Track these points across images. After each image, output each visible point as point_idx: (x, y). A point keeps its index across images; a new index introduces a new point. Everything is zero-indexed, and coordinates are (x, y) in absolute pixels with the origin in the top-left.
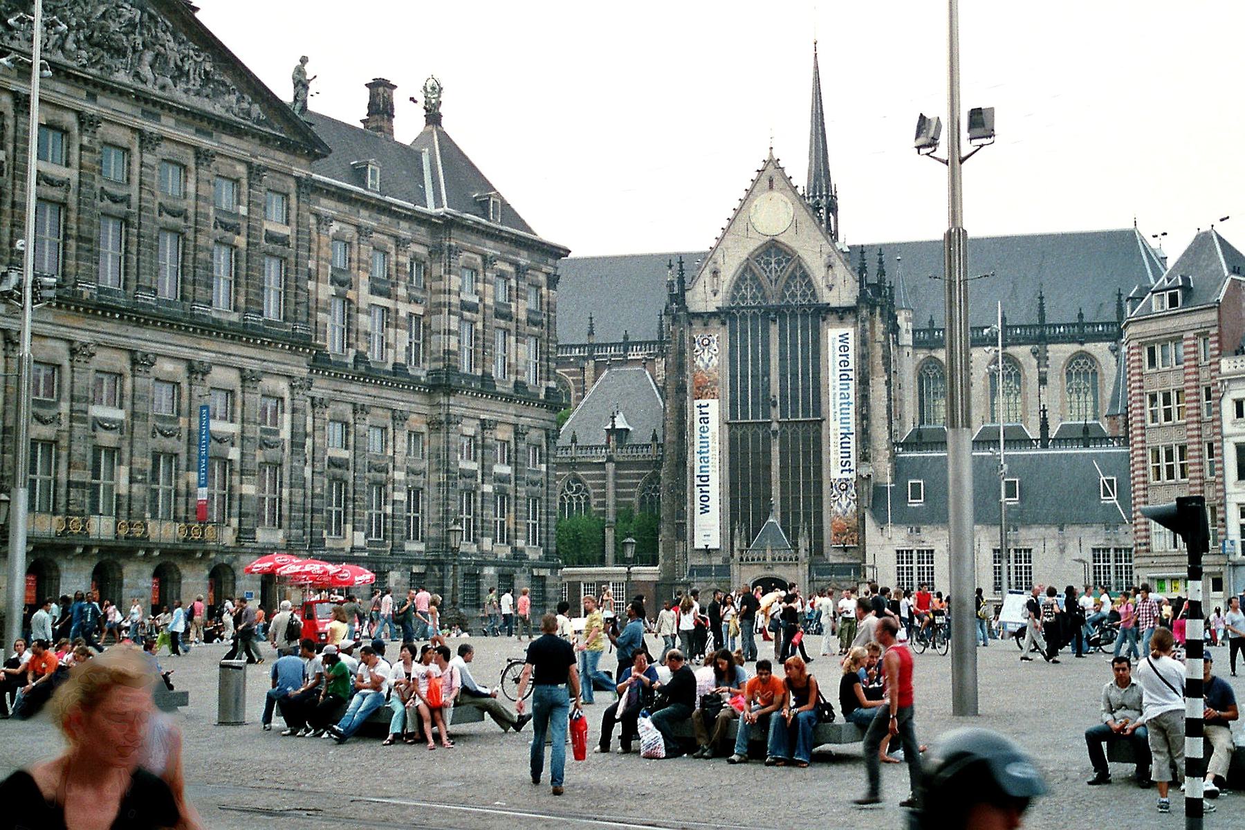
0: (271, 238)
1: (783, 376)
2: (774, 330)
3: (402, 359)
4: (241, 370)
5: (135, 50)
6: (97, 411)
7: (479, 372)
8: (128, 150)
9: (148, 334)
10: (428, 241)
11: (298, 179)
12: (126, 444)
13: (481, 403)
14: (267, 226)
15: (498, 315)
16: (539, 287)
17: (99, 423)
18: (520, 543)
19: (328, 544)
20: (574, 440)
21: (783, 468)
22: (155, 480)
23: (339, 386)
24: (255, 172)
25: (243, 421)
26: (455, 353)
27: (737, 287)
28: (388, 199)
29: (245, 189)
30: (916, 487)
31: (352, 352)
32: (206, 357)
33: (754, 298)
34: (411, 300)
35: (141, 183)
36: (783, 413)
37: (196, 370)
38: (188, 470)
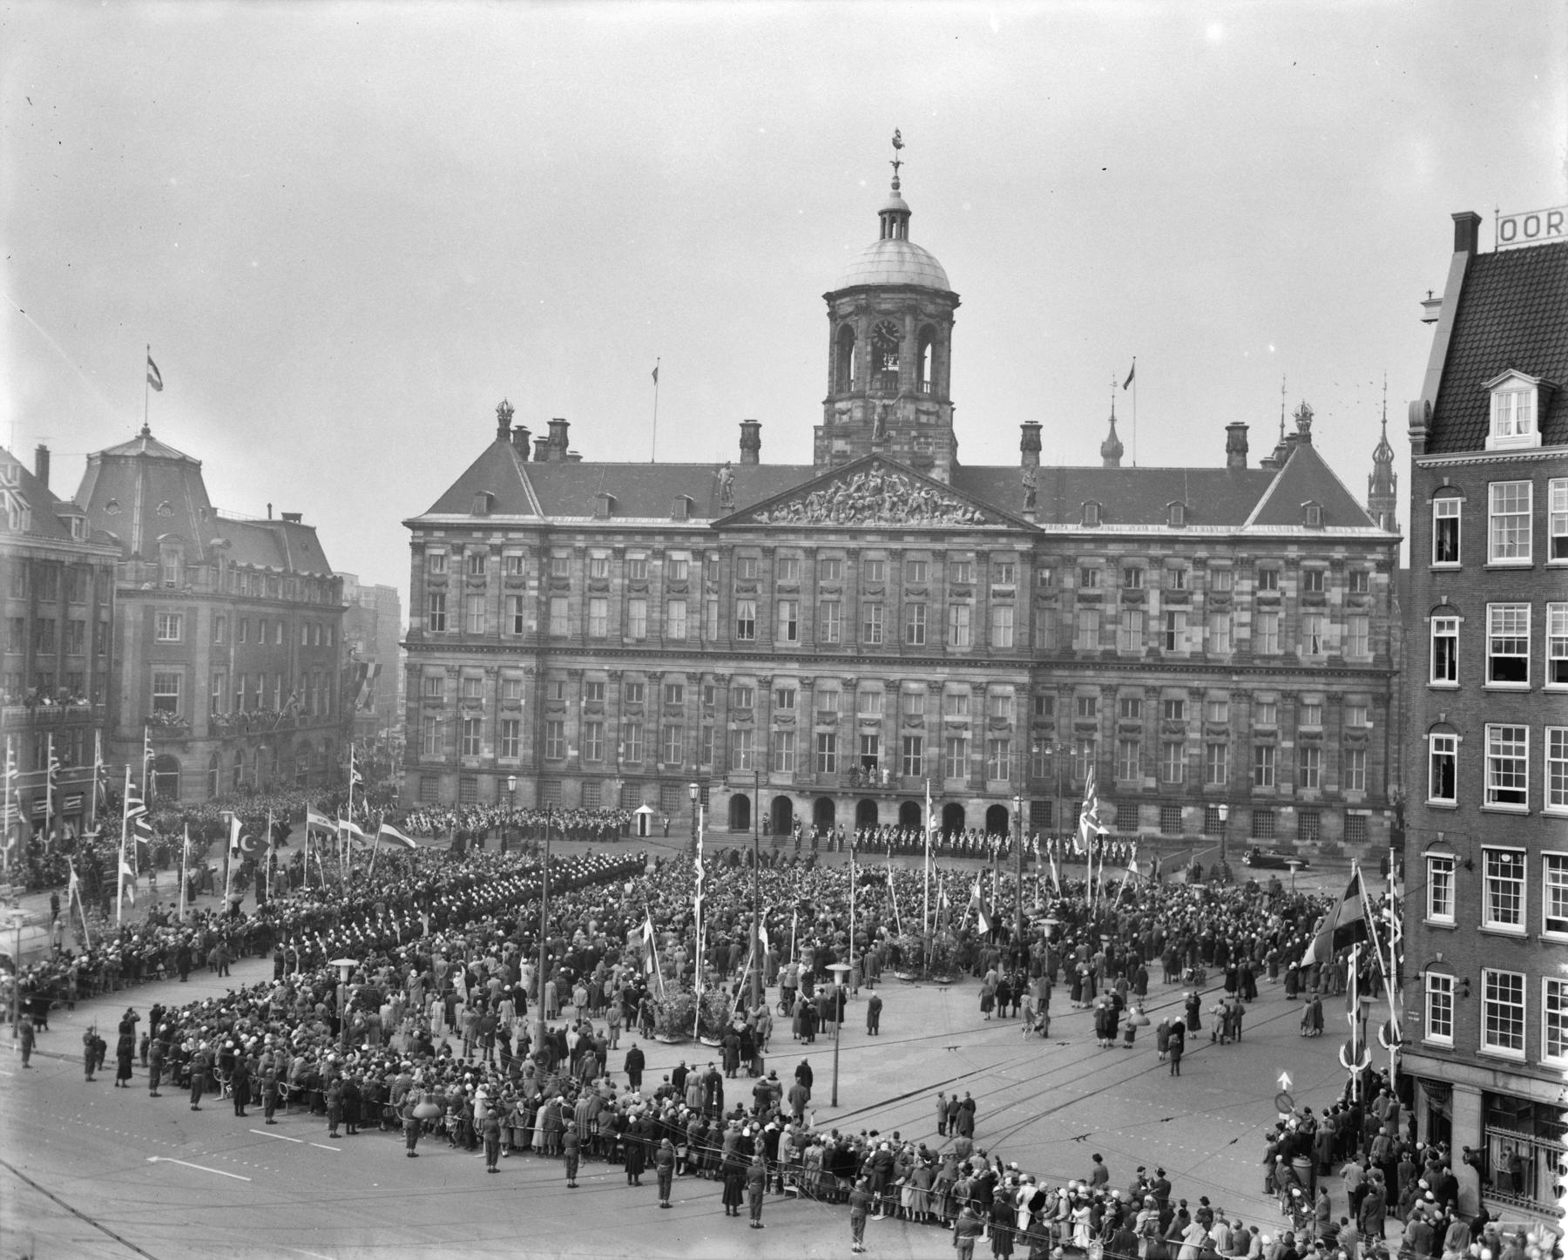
0: (996, 594)
3: (1199, 648)
6: (860, 715)
7: (1281, 652)
9: (896, 668)
11: (1022, 554)
13: (1278, 678)
14: (995, 587)
15: (1305, 603)
16: (1365, 573)
17: (863, 722)
18: (1333, 788)
19: (1119, 786)
22: (907, 751)
23: (1128, 674)
24: (983, 556)
25: (975, 715)
26: (1249, 641)
31: (1144, 650)
37: (936, 688)
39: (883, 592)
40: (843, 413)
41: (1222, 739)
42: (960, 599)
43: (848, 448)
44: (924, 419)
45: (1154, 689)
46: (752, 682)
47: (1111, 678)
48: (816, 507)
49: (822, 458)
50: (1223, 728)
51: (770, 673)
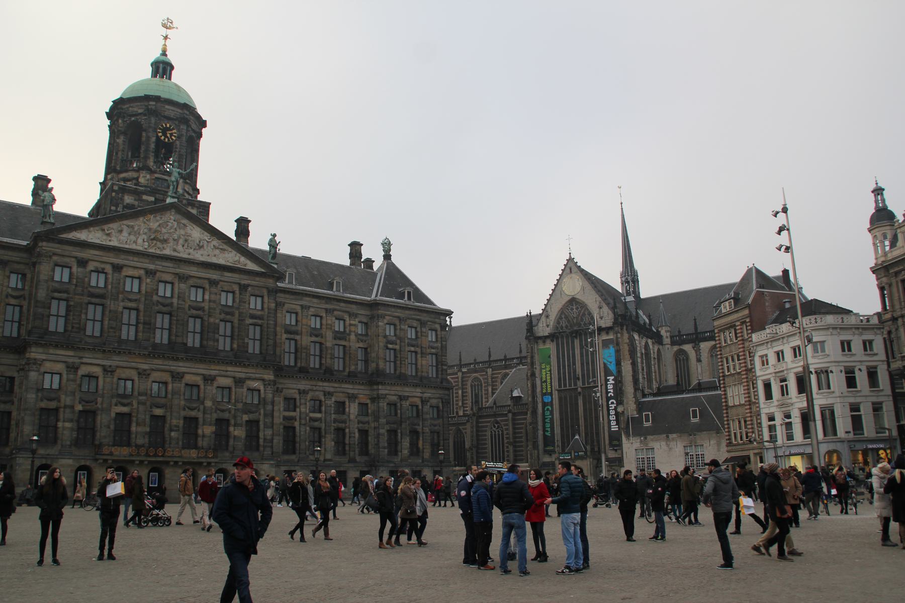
0: (253, 317)
1: (582, 364)
2: (577, 342)
4: (234, 378)
5: (174, 240)
8: (172, 284)
9: (181, 364)
10: (368, 313)
12: (168, 414)
20: (495, 403)
21: (585, 410)
23: (314, 383)
27: (558, 323)
28: (346, 295)
29: (237, 295)
30: (647, 416)
32: (213, 373)
33: (567, 327)
34: (358, 341)
35: (179, 297)
36: (584, 383)
37: (209, 379)
38: (204, 424)
39: (171, 304)
40: (129, 180)
41: (366, 427)
42: (228, 317)
43: (136, 203)
44: (187, 196)
45: (329, 393)
46: (60, 367)
47: (303, 385)
48: (125, 234)
49: (117, 206)
50: (366, 419)
51: (77, 361)
